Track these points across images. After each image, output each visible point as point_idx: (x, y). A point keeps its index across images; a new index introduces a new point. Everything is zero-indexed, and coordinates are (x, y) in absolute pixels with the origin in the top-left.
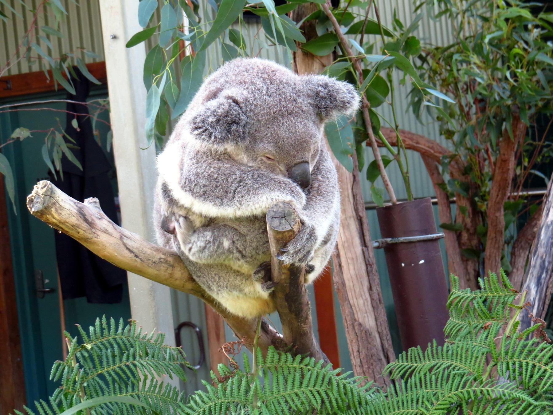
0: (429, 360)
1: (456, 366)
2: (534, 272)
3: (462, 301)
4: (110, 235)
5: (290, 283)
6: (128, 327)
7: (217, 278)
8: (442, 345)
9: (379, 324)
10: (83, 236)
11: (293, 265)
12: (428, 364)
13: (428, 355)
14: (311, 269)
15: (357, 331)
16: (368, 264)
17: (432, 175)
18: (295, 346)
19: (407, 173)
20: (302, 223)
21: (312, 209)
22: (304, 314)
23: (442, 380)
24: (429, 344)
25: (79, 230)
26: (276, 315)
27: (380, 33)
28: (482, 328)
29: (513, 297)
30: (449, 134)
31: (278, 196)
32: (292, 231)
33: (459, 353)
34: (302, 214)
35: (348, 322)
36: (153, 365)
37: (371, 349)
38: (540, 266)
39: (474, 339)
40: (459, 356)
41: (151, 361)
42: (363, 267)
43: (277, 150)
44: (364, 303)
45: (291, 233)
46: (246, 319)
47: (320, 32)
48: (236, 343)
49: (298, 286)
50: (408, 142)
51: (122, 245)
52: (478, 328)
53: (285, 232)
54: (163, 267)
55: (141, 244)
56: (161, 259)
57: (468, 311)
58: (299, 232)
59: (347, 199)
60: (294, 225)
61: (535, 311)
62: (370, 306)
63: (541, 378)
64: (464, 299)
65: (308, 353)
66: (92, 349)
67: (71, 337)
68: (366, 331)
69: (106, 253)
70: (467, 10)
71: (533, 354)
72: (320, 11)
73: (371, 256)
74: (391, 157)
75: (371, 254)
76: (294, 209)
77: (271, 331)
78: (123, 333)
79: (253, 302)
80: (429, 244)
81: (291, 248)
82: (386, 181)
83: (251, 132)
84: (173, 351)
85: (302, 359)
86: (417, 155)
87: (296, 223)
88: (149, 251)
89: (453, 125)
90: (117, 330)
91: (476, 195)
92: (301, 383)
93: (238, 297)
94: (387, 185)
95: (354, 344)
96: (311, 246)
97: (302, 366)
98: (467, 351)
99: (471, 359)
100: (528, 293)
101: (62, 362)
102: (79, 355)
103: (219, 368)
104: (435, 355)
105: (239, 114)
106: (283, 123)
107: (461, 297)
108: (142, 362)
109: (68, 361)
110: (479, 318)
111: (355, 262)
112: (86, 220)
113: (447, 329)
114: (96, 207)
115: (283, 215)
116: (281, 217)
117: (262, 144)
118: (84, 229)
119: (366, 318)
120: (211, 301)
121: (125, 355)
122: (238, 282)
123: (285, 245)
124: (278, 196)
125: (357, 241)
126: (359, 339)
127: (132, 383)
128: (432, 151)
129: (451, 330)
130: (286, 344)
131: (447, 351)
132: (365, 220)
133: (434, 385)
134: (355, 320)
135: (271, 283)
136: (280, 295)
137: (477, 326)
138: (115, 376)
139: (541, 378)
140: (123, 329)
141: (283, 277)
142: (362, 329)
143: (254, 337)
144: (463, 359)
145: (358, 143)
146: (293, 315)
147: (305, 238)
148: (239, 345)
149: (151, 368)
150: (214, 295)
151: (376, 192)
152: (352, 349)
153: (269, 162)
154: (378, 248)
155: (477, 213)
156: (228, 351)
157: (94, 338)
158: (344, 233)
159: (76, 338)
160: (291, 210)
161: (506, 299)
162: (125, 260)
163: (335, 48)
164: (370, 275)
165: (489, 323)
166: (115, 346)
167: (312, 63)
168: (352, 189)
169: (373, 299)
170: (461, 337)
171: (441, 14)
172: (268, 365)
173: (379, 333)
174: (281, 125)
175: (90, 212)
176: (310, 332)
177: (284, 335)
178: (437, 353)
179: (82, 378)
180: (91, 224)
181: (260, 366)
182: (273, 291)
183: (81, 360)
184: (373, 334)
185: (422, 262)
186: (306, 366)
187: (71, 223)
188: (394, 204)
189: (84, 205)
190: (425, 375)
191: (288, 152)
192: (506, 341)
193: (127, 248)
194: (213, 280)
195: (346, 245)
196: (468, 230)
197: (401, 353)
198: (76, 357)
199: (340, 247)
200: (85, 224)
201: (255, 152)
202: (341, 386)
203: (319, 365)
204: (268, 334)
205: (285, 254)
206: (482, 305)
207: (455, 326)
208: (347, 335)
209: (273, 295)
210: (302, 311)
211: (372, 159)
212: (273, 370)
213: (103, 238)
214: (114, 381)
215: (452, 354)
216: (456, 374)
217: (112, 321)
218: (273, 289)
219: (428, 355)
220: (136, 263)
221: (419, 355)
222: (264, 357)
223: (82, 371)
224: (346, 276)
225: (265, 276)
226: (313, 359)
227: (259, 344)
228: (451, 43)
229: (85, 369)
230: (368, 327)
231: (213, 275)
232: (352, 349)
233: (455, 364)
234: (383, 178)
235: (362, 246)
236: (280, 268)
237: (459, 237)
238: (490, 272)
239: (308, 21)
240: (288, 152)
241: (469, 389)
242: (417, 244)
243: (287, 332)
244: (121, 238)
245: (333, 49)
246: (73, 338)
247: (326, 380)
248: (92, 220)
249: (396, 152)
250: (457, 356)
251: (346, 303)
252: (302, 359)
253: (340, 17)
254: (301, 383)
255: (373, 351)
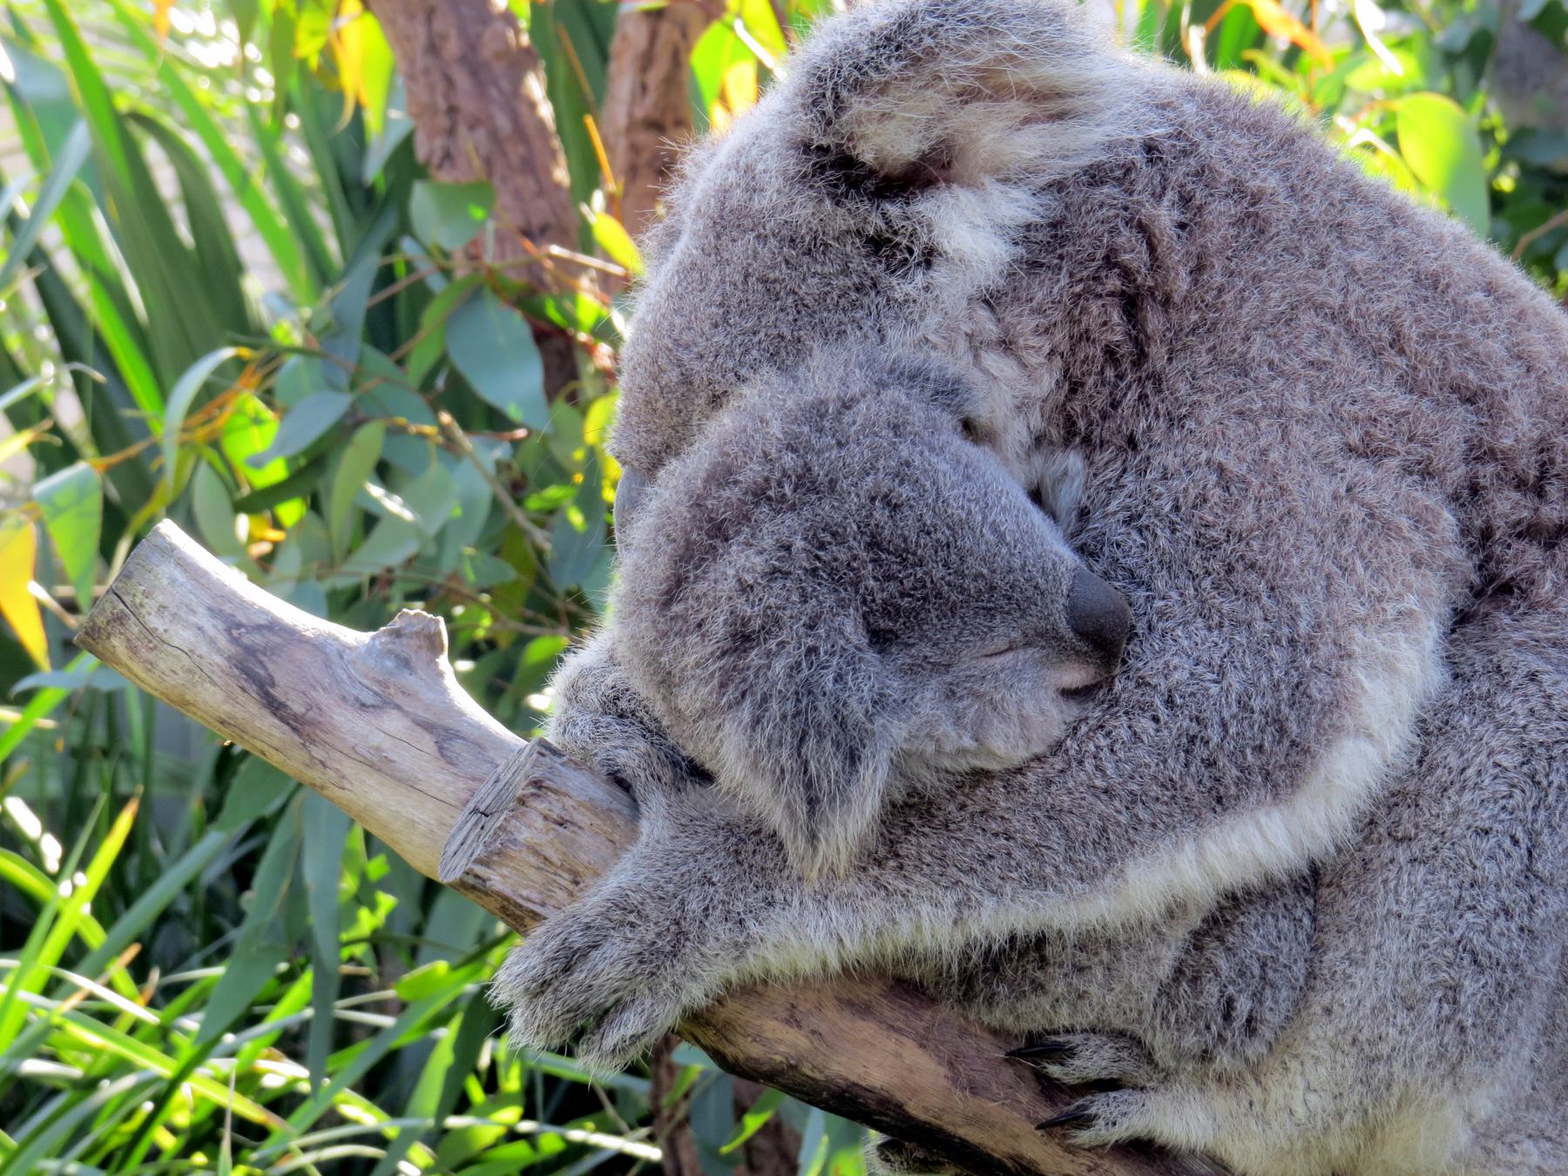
4: (409, 784)
118: (275, 743)
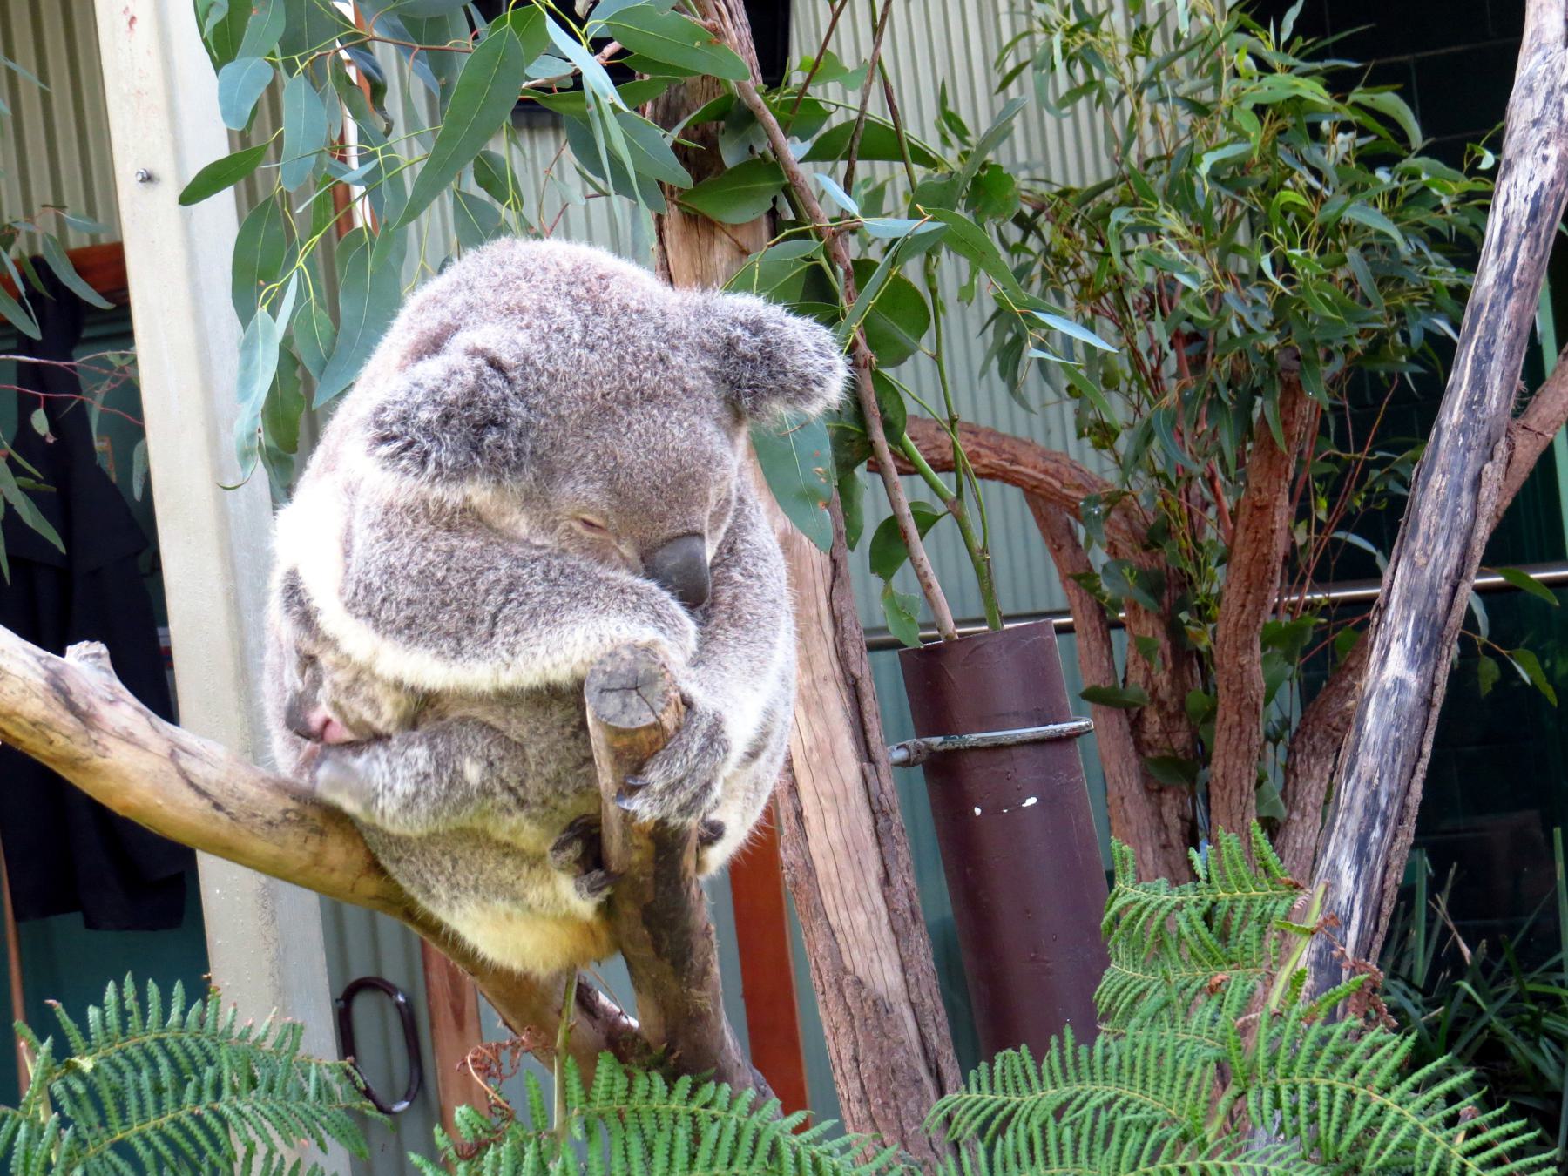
0: (1055, 1085)
1: (1130, 1101)
2: (1348, 823)
3: (1145, 914)
4: (141, 746)
5: (657, 876)
6: (197, 1006)
7: (447, 863)
8: (1091, 1045)
9: (912, 980)
10: (63, 753)
11: (662, 823)
12: (1052, 1095)
13: (1051, 1072)
14: (714, 833)
15: (849, 1002)
16: (878, 812)
17: (1057, 550)
18: (673, 1051)
19: (985, 550)
20: (688, 704)
21: (714, 665)
22: (697, 961)
23: (1091, 1140)
24: (1054, 1040)
25: (53, 736)
26: (618, 963)
27: (902, 158)
28: (1200, 989)
29: (1288, 901)
30: (1104, 435)
31: (618, 629)
32: (658, 727)
33: (1139, 1063)
34: (687, 678)
35: (825, 978)
36: (270, 1114)
37: (891, 1052)
38: (1366, 809)
39: (1179, 1024)
40: (1138, 1069)
41: (264, 1103)
42: (866, 820)
43: (614, 502)
44: (869, 922)
45: (654, 734)
46: (533, 977)
47: (730, 157)
48: (505, 1047)
49: (678, 883)
50: (989, 458)
51: (177, 776)
52: (1191, 991)
53: (638, 730)
54: (293, 836)
55: (229, 772)
56: (286, 811)
57: (1160, 944)
58: (678, 729)
59: (815, 629)
60: (663, 711)
61: (1352, 935)
62: (886, 929)
63: (1370, 1130)
64: (1149, 909)
65: (713, 1071)
66: (95, 1070)
67: (34, 1039)
68: (875, 1002)
69: (130, 800)
70: (1149, 83)
71: (1349, 1062)
72: (730, 97)
73: (887, 788)
74: (940, 508)
75: (888, 784)
76: (663, 666)
77: (604, 1008)
78: (183, 1024)
79: (552, 929)
80: (1050, 750)
81: (655, 777)
82: (926, 574)
83: (540, 452)
84: (326, 1071)
85: (695, 1088)
86: (1014, 493)
87: (668, 704)
88: (253, 792)
89: (1117, 410)
90: (166, 1014)
91: (1182, 605)
92: (693, 1157)
93: (509, 917)
94: (930, 586)
95: (842, 1040)
96: (715, 769)
97: (694, 1107)
98: (1161, 1055)
99: (1174, 1079)
100: (1331, 888)
101: (10, 1111)
102: (58, 1088)
103: (457, 1117)
104: (1071, 1071)
105: (505, 400)
106: (630, 424)
107: (1141, 903)
108: (239, 1105)
109: (27, 1106)
110: (1194, 963)
111: (842, 808)
112: (72, 707)
113: (1103, 994)
114: (100, 668)
115: (631, 683)
116: (626, 689)
117: (571, 484)
118: (68, 733)
119: (877, 965)
120: (433, 928)
121: (191, 1087)
122: (507, 873)
123: (638, 768)
124: (618, 629)
125: (846, 745)
126: (857, 1023)
127: (212, 1164)
128: (1057, 485)
129: (1115, 998)
130: (648, 1048)
131: (1106, 1058)
132: (867, 687)
133: (1068, 1155)
134: (845, 971)
135: (601, 874)
136: (628, 909)
137: (1188, 986)
138: (163, 1148)
139: (1370, 1130)
140: (184, 1013)
141: (636, 857)
142: (864, 994)
143: (557, 1027)
144: (1151, 1081)
145: (845, 468)
146: (666, 965)
147: (695, 746)
148: (514, 1053)
149: (266, 1123)
150: (441, 913)
151: (898, 607)
152: (838, 1053)
153: (589, 535)
154: (906, 764)
155: (1185, 656)
156: (485, 1070)
157: (102, 1040)
158: (809, 723)
159: (49, 1040)
160: (655, 669)
161: (1269, 907)
162: (186, 818)
163: (775, 200)
164: (884, 841)
165: (1221, 976)
166: (163, 1062)
167: (711, 245)
168: (830, 599)
169: (895, 911)
170: (1144, 1018)
171: (1074, 94)
172: (598, 1105)
173: (913, 1005)
174: (623, 430)
175: (83, 683)
176: (715, 1011)
177: (643, 1019)
178: (1076, 1064)
179: (70, 1154)
180: (85, 718)
181: (576, 1111)
182: (609, 899)
183: (65, 1103)
184: (896, 1008)
185: (1031, 801)
186: (706, 1106)
187: (31, 717)
188: (949, 638)
189: (65, 665)
190: (1043, 1128)
191: (645, 507)
192: (1270, 1026)
193: (191, 785)
194: (436, 870)
195: (815, 758)
196: (1161, 705)
197: (975, 1066)
198: (51, 1095)
199: (797, 764)
200: (70, 717)
201: (549, 507)
202: (807, 1163)
203: (742, 1105)
204: (596, 1018)
205: (641, 793)
206: (1200, 925)
207: (1125, 986)
208: (822, 1013)
209: (607, 910)
210: (691, 949)
211: (887, 512)
212: (613, 1122)
213: (120, 758)
214: (159, 1159)
215: (1120, 1066)
216: (1130, 1122)
217: (153, 989)
218: (607, 891)
219: (1051, 1072)
220: (215, 828)
221: (1025, 1072)
222: (587, 1083)
223: (67, 1134)
224: (817, 846)
225: (584, 854)
226: (726, 1087)
227: (570, 1048)
228: (1107, 175)
229: (76, 1128)
230: (881, 989)
231: (438, 856)
232: (838, 1053)
233: (1127, 1094)
234: (917, 567)
235: (861, 760)
236: (625, 834)
237: (1137, 724)
238: (1221, 831)
239: (696, 127)
240: (645, 507)
241: (1169, 1166)
242: (1015, 752)
243: (651, 1012)
244: (173, 756)
245: (770, 205)
246: (42, 1040)
247: (764, 1145)
248: (90, 705)
249: (953, 494)
250: (1133, 1071)
251: (819, 921)
252: (695, 1088)
253: (786, 114)
254: (693, 1157)
255: (897, 1057)
